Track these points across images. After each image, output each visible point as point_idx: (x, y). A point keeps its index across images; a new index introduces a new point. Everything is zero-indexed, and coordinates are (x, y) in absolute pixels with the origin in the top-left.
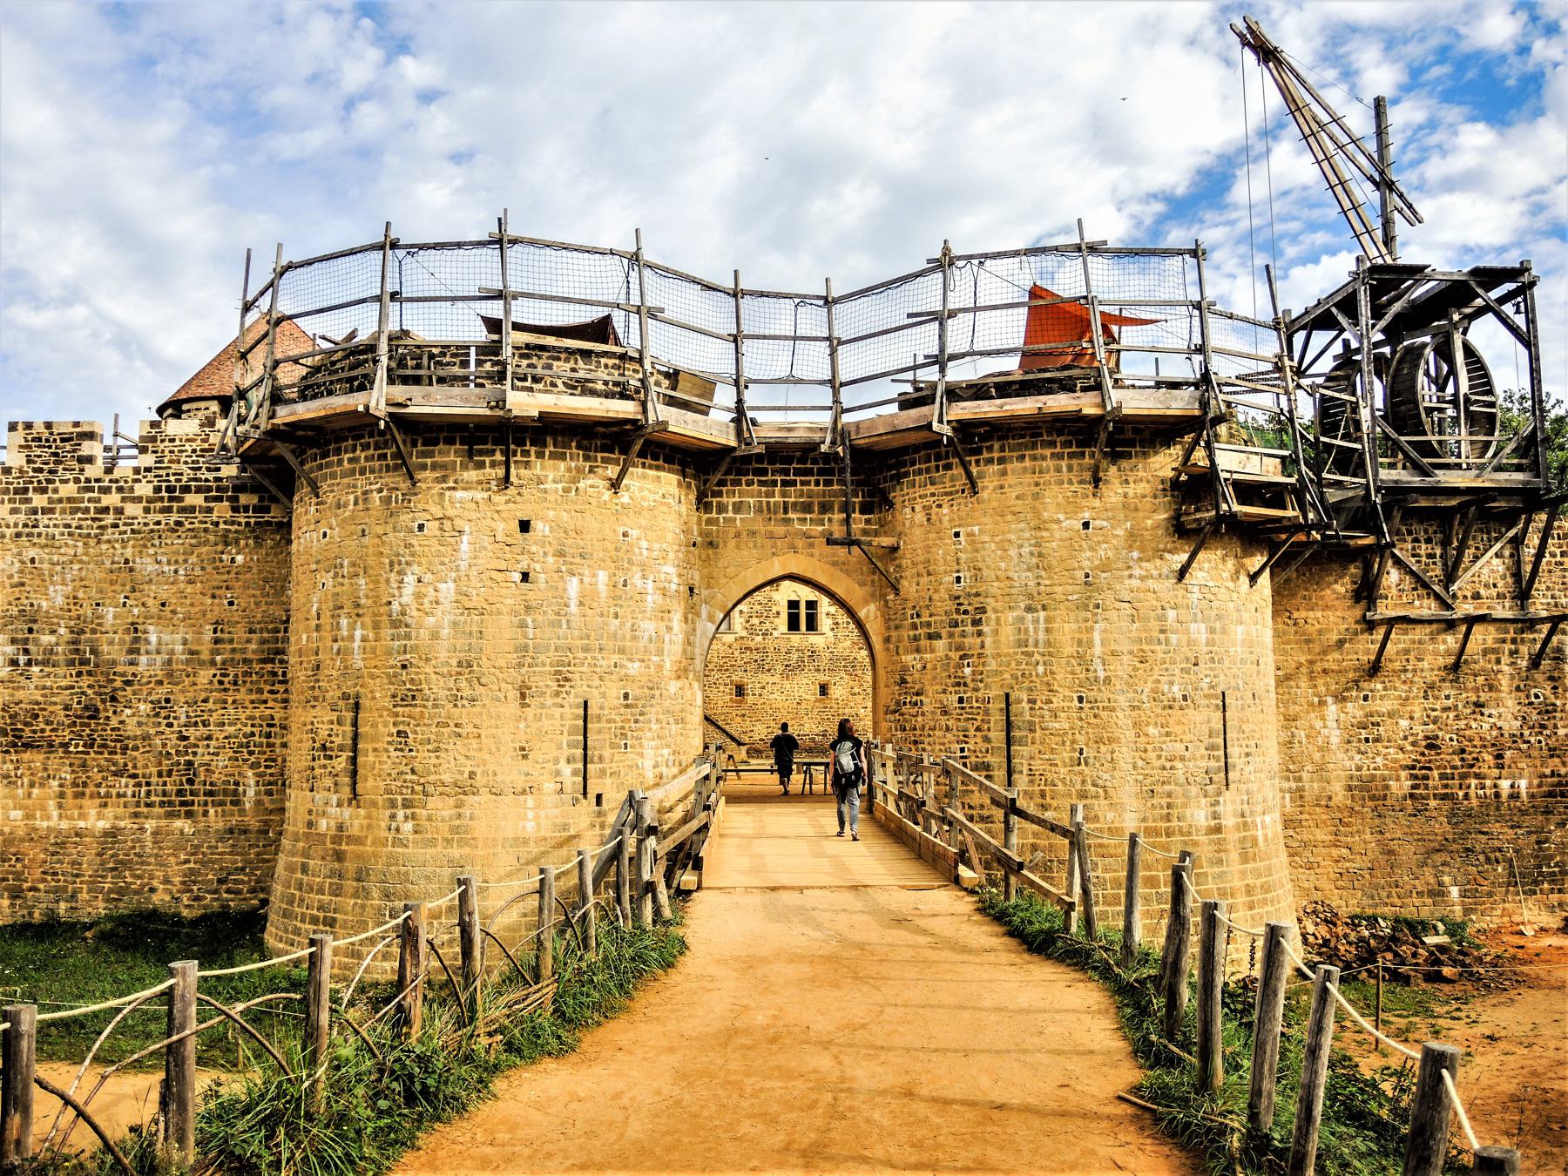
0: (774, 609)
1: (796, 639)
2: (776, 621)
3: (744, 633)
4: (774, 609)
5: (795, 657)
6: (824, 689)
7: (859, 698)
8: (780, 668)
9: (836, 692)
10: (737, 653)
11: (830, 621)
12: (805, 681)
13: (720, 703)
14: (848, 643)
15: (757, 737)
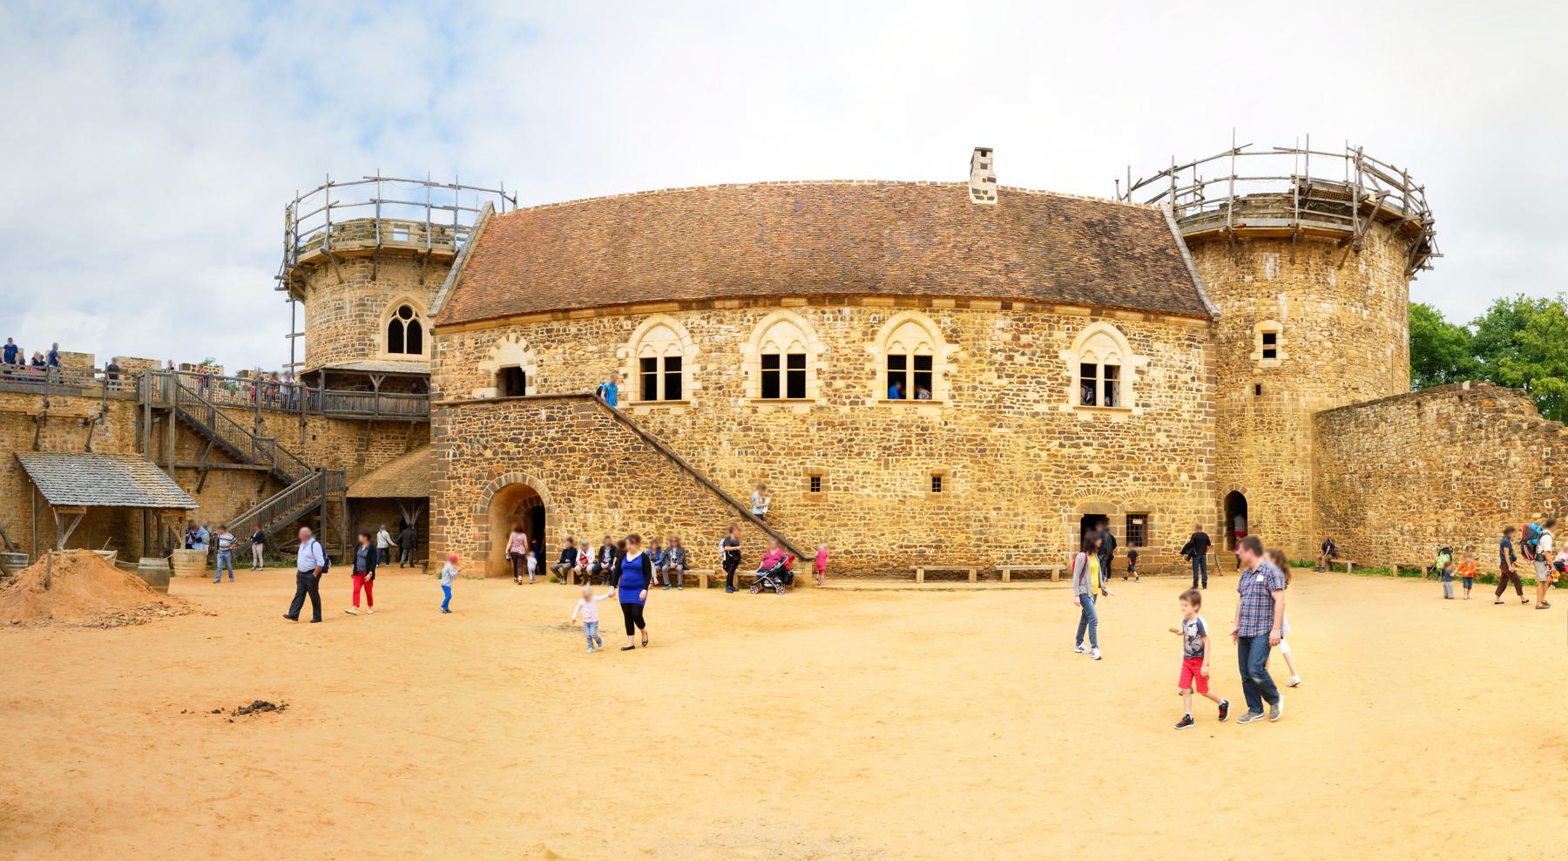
0: (868, 367)
1: (898, 410)
2: (870, 384)
3: (823, 402)
4: (868, 367)
5: (897, 435)
6: (937, 482)
7: (990, 496)
8: (875, 451)
9: (959, 486)
10: (813, 430)
11: (948, 385)
12: (912, 470)
13: (789, 501)
14: (975, 417)
15: (840, 548)
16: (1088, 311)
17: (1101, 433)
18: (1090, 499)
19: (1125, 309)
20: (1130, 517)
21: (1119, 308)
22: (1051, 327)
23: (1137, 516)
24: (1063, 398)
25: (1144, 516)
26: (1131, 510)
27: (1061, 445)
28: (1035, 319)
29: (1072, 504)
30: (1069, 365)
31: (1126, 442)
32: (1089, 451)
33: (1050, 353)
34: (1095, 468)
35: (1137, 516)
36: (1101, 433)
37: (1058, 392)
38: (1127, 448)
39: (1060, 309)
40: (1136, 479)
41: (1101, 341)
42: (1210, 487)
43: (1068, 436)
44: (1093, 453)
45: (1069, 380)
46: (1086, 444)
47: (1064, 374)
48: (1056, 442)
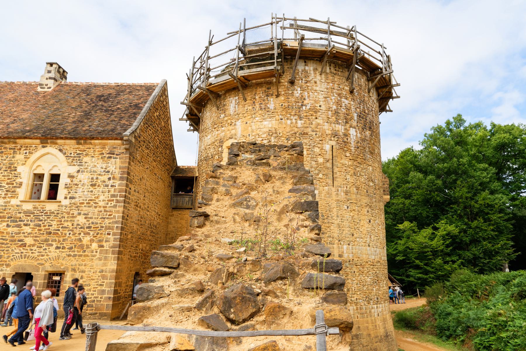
16: (38, 141)
17: (37, 217)
18: (22, 262)
19: (62, 138)
20: (52, 274)
21: (57, 138)
22: (14, 152)
23: (57, 274)
24: (14, 195)
25: (61, 274)
26: (50, 269)
27: (8, 226)
28: (5, 148)
29: (8, 265)
30: (22, 176)
31: (54, 223)
32: (28, 229)
33: (12, 168)
34: (29, 241)
35: (57, 274)
36: (37, 217)
37: (12, 192)
38: (55, 227)
39: (21, 141)
40: (58, 248)
41: (51, 159)
42: (113, 253)
43: (15, 221)
44: (29, 231)
45: (21, 184)
46: (26, 225)
47: (18, 180)
48: (5, 224)
